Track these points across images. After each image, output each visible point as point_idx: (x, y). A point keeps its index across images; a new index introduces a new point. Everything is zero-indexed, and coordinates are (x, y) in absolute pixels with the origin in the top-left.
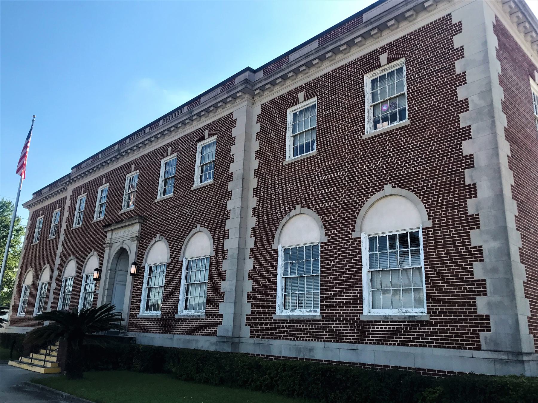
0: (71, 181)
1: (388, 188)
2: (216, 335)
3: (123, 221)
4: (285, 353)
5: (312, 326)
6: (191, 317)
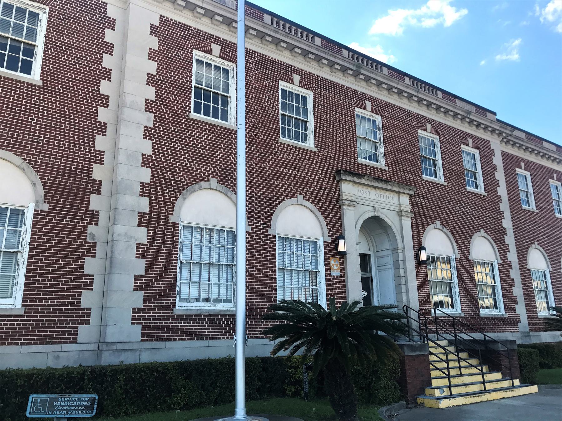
0: (505, 140)
1: (300, 197)
2: (518, 331)
3: (389, 182)
4: (549, 340)
5: (252, 322)
6: (496, 316)
